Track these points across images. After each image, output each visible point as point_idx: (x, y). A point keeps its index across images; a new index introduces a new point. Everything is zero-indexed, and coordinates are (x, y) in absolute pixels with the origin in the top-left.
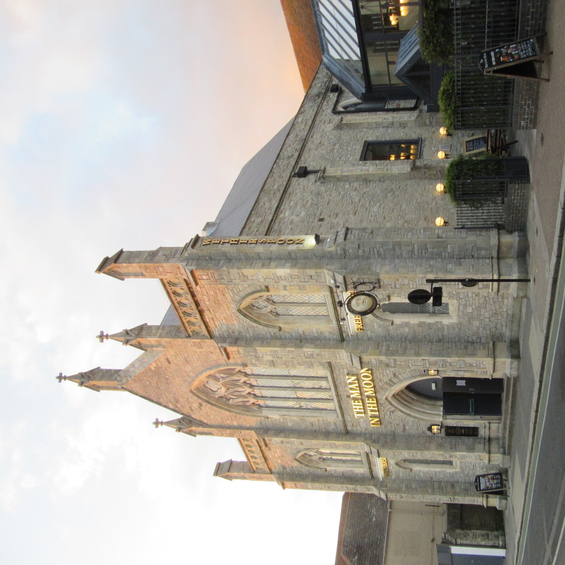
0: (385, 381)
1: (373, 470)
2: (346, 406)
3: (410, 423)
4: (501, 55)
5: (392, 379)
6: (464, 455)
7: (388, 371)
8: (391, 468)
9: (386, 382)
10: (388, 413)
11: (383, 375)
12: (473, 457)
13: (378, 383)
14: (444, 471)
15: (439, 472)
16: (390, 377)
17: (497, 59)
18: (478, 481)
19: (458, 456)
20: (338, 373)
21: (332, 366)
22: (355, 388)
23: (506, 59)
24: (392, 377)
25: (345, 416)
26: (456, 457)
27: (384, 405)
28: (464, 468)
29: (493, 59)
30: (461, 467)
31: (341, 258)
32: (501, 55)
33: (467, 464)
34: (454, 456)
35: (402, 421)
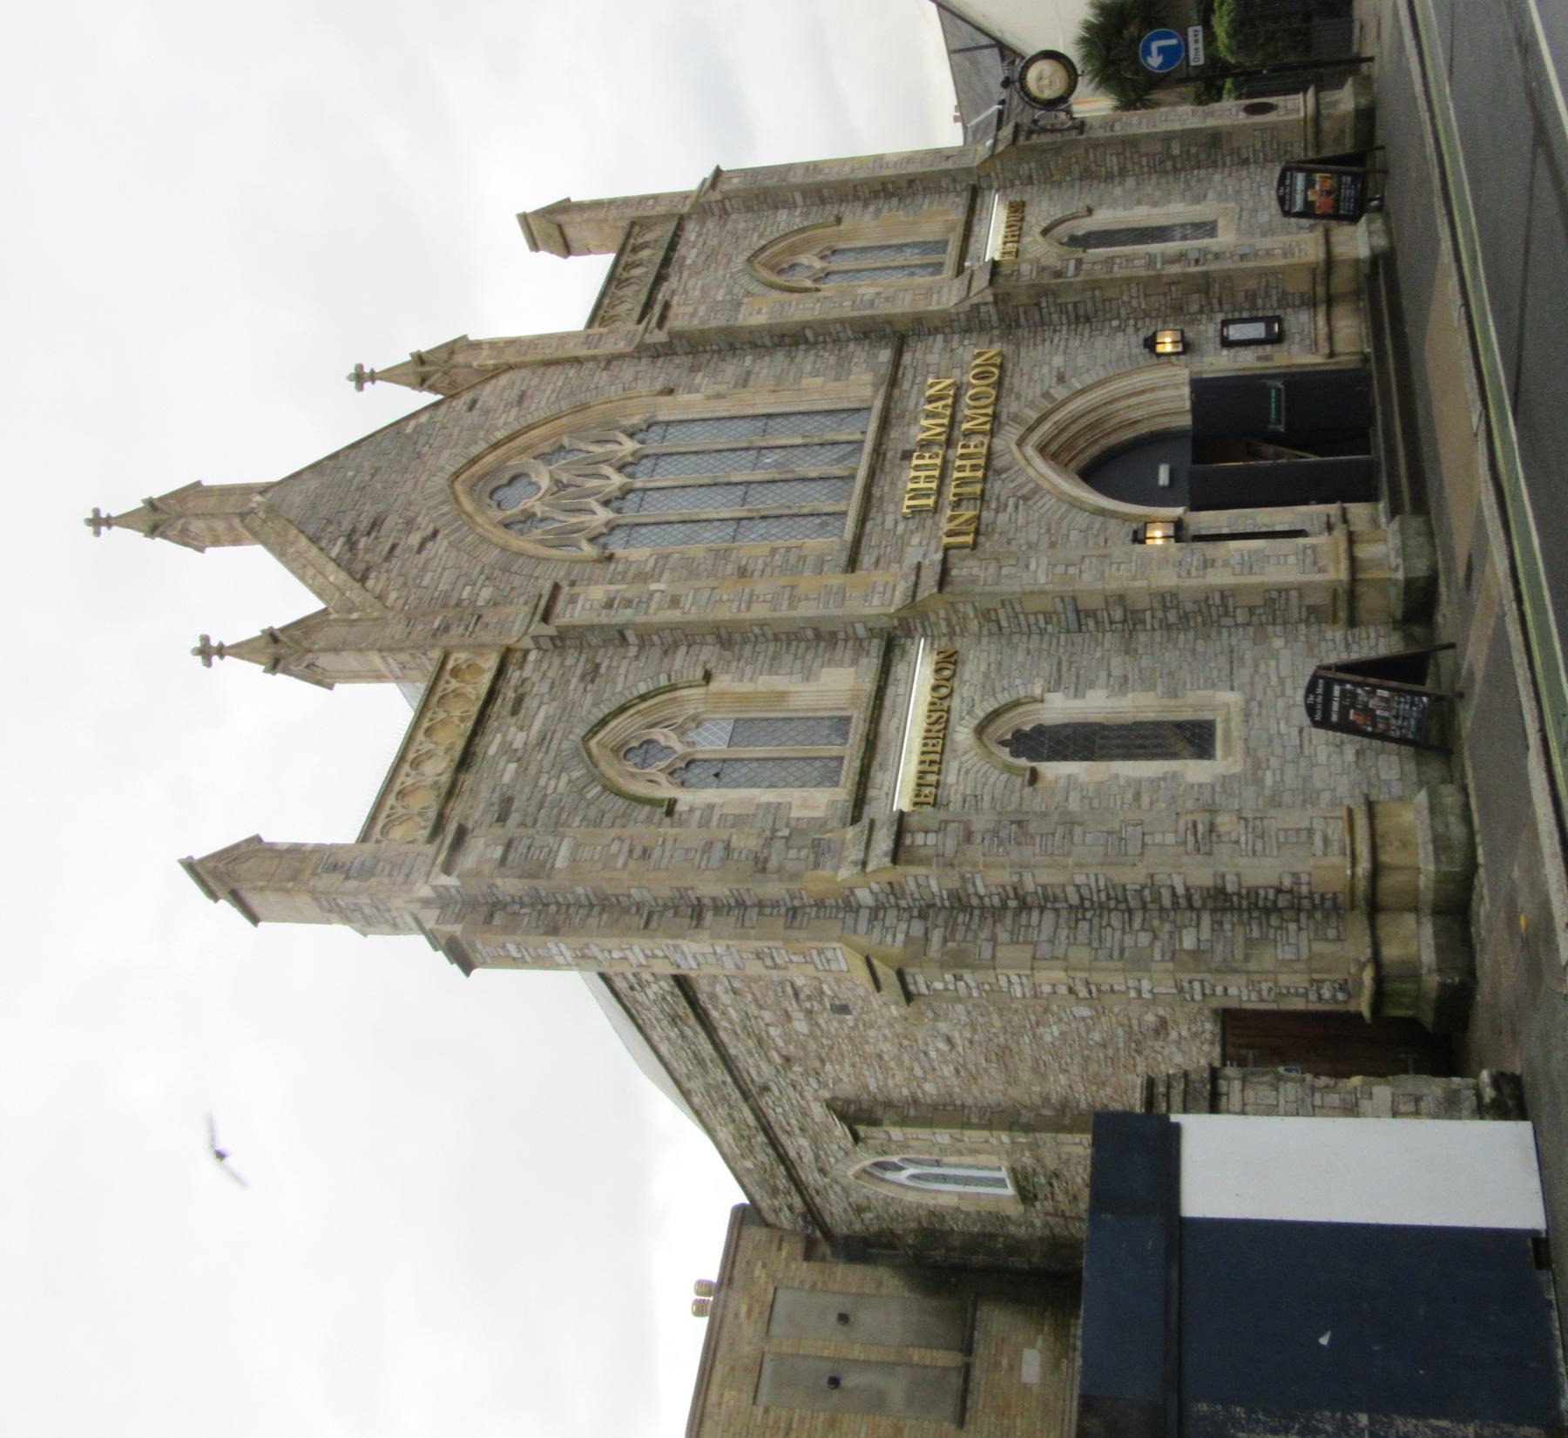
0: (1030, 397)
1: (872, 793)
2: (886, 489)
3: (1074, 535)
4: (1353, 706)
5: (1052, 391)
6: (1257, 552)
7: (1045, 370)
8: (951, 779)
9: (1032, 402)
10: (1011, 501)
11: (1030, 379)
12: (1292, 560)
13: (1009, 405)
14: (1174, 775)
15: (1151, 781)
16: (1047, 384)
17: (1344, 711)
18: (1320, 691)
19: (1236, 559)
20: (906, 386)
21: (901, 369)
22: (940, 410)
23: (1360, 720)
24: (1054, 381)
25: (869, 525)
26: (1226, 564)
27: (1004, 476)
28: (1261, 753)
29: (1335, 706)
30: (1248, 751)
31: (1005, 188)
32: (1353, 706)
33: (1273, 731)
34: (1219, 563)
35: (1048, 531)
